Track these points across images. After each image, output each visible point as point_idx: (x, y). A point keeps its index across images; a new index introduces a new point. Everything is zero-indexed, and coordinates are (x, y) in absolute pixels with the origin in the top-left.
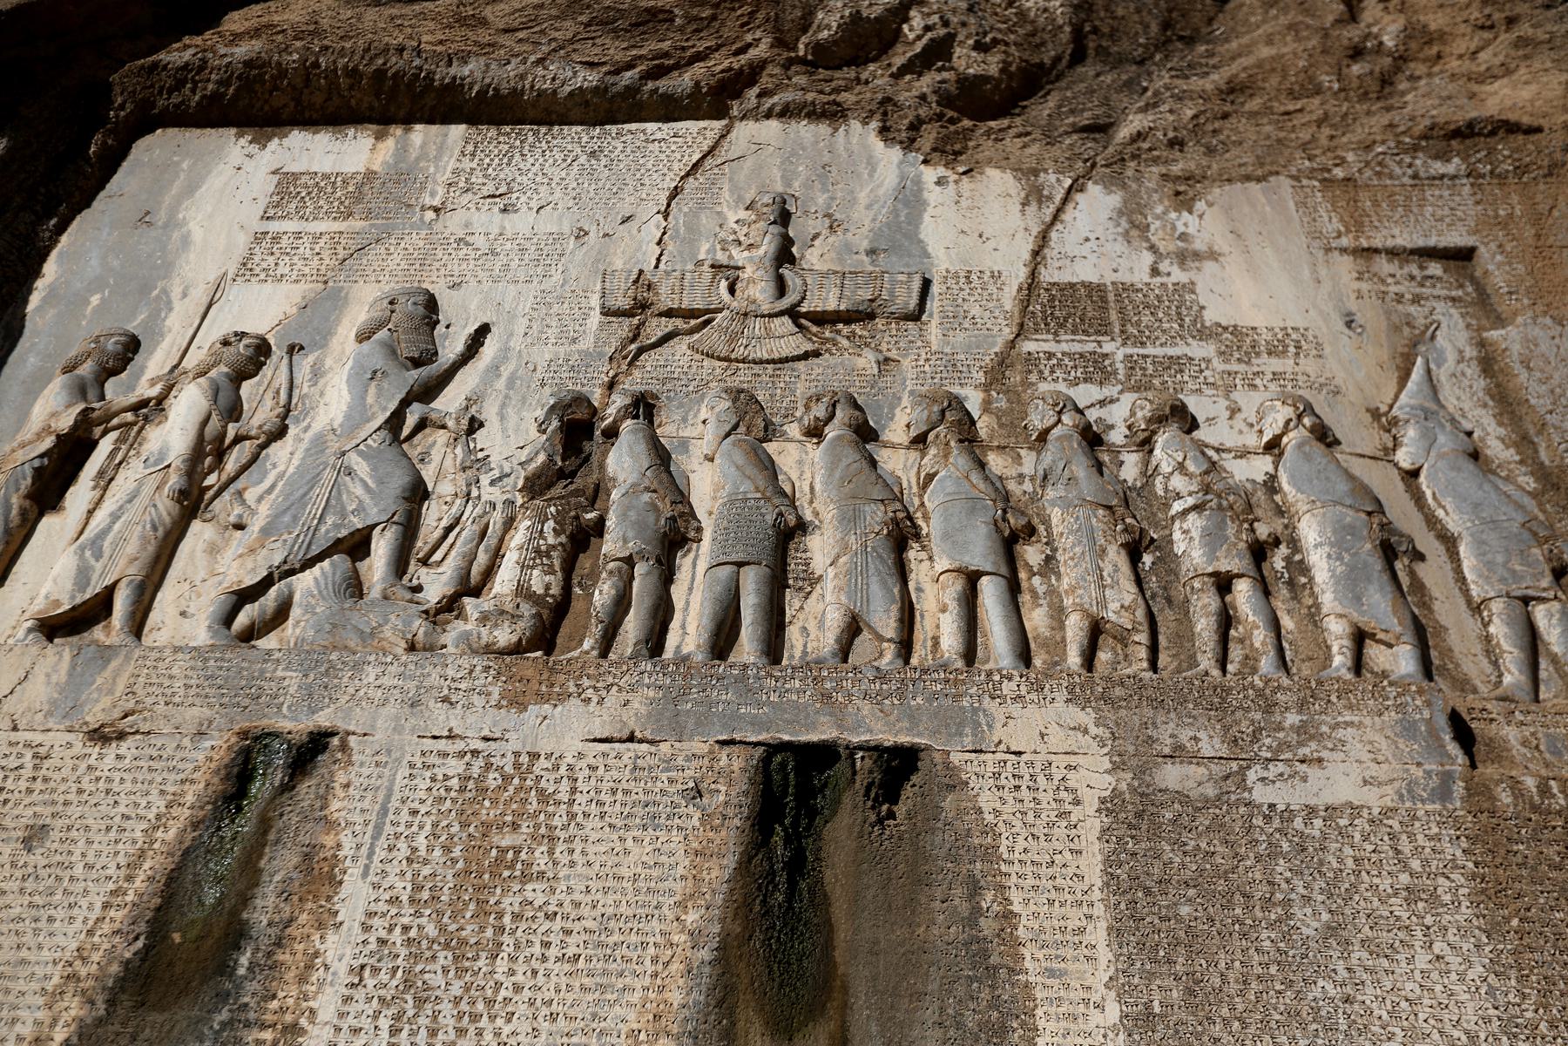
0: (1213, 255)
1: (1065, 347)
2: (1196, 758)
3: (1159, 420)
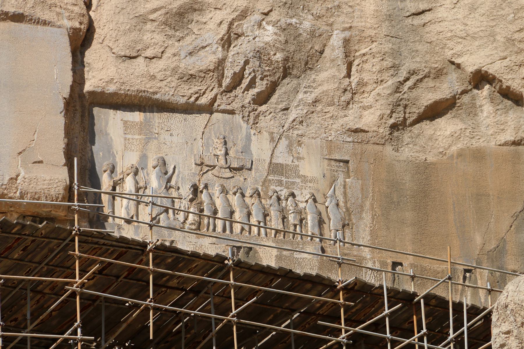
0: (303, 158)
3: (289, 196)
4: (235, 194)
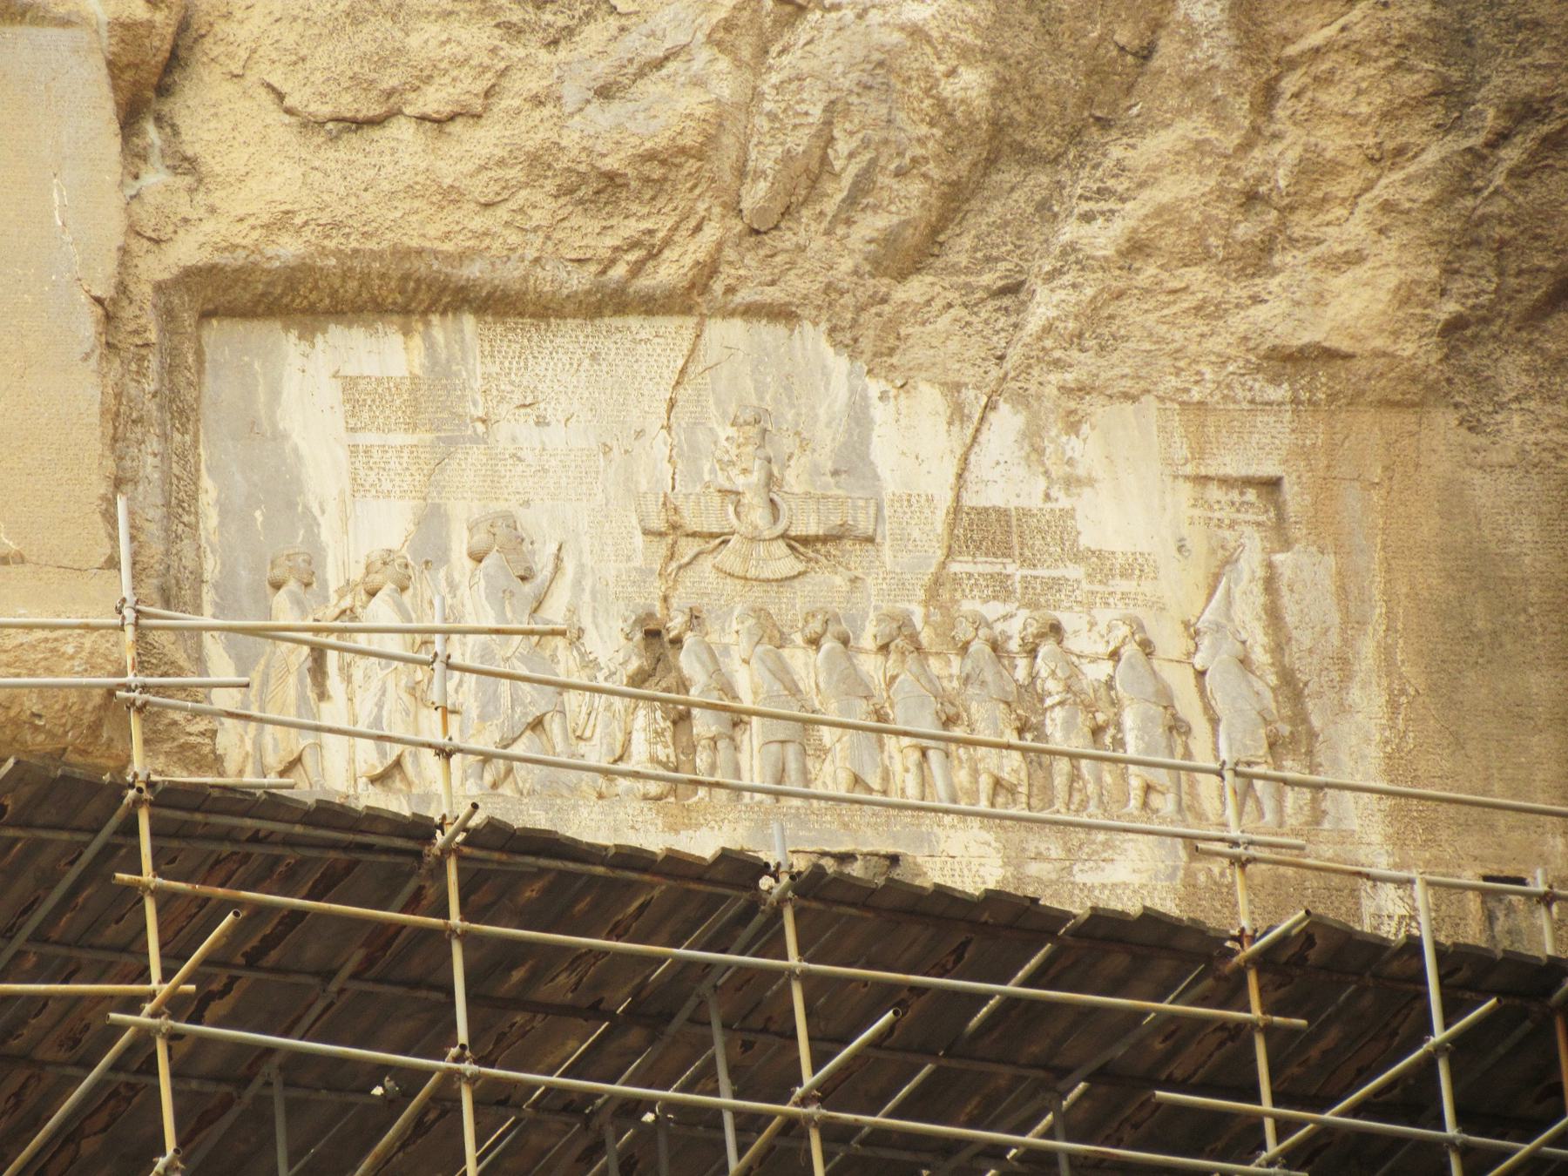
0: (1090, 482)
1: (980, 568)
2: (1048, 859)
4: (815, 642)
